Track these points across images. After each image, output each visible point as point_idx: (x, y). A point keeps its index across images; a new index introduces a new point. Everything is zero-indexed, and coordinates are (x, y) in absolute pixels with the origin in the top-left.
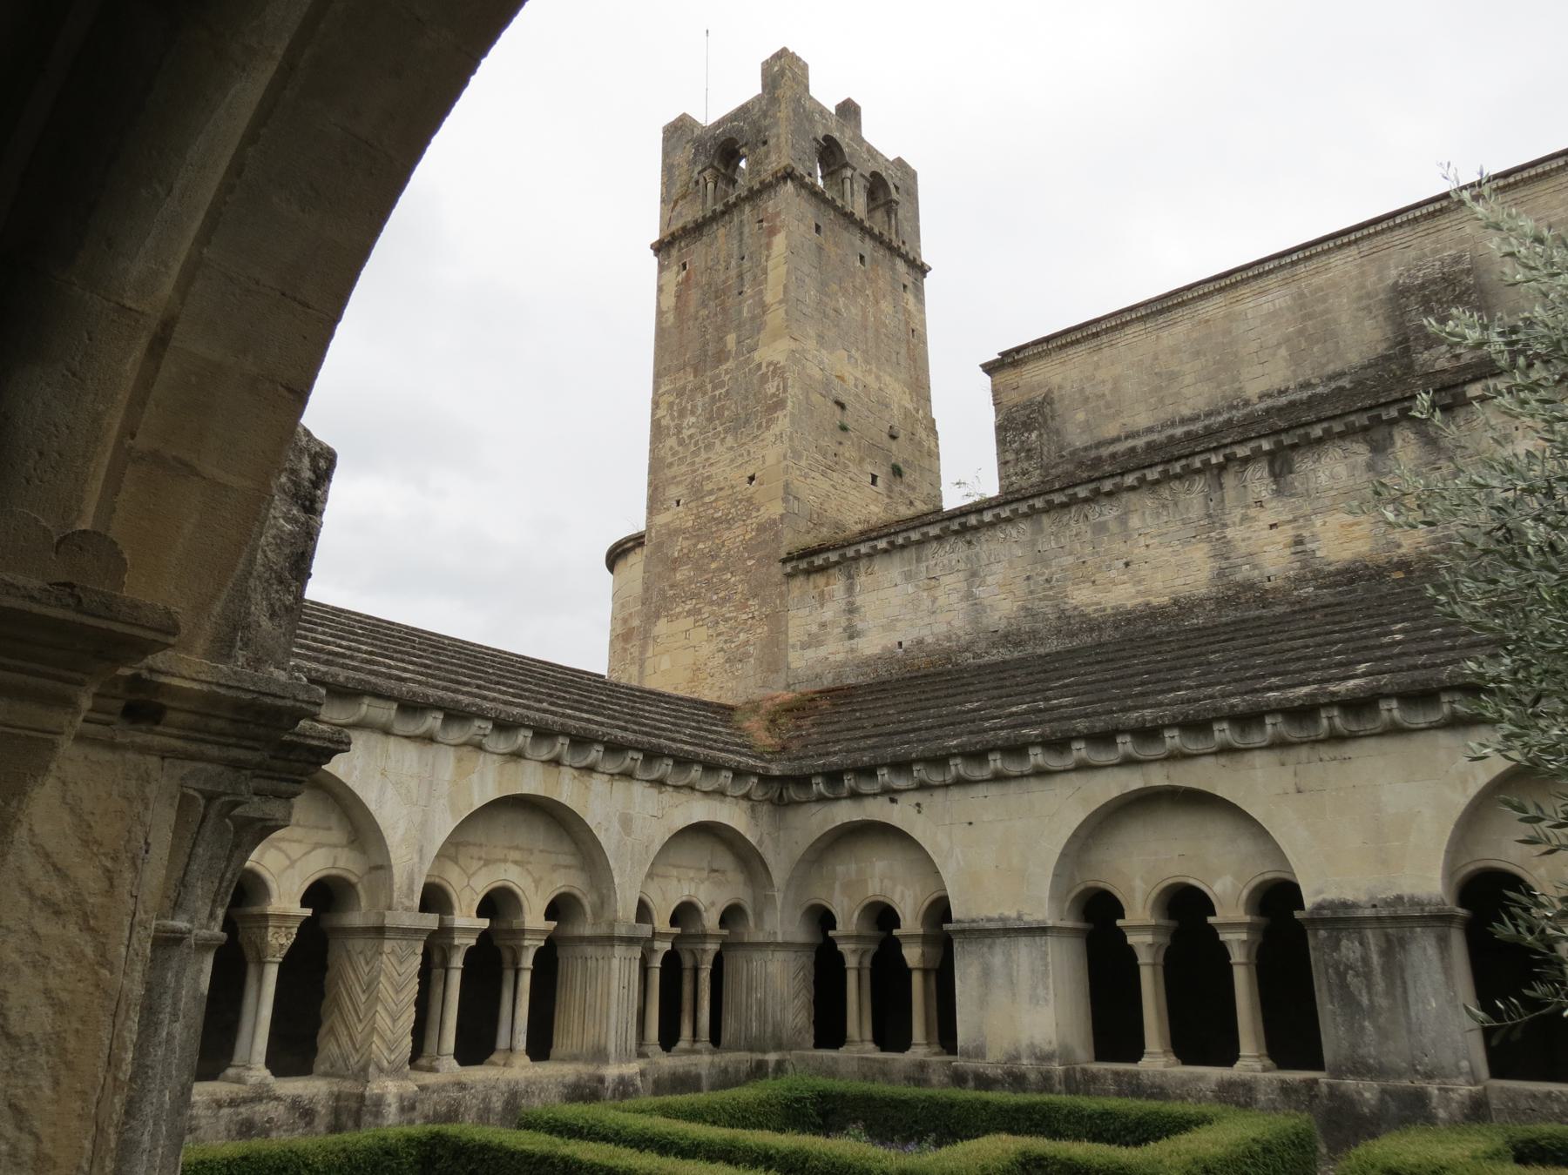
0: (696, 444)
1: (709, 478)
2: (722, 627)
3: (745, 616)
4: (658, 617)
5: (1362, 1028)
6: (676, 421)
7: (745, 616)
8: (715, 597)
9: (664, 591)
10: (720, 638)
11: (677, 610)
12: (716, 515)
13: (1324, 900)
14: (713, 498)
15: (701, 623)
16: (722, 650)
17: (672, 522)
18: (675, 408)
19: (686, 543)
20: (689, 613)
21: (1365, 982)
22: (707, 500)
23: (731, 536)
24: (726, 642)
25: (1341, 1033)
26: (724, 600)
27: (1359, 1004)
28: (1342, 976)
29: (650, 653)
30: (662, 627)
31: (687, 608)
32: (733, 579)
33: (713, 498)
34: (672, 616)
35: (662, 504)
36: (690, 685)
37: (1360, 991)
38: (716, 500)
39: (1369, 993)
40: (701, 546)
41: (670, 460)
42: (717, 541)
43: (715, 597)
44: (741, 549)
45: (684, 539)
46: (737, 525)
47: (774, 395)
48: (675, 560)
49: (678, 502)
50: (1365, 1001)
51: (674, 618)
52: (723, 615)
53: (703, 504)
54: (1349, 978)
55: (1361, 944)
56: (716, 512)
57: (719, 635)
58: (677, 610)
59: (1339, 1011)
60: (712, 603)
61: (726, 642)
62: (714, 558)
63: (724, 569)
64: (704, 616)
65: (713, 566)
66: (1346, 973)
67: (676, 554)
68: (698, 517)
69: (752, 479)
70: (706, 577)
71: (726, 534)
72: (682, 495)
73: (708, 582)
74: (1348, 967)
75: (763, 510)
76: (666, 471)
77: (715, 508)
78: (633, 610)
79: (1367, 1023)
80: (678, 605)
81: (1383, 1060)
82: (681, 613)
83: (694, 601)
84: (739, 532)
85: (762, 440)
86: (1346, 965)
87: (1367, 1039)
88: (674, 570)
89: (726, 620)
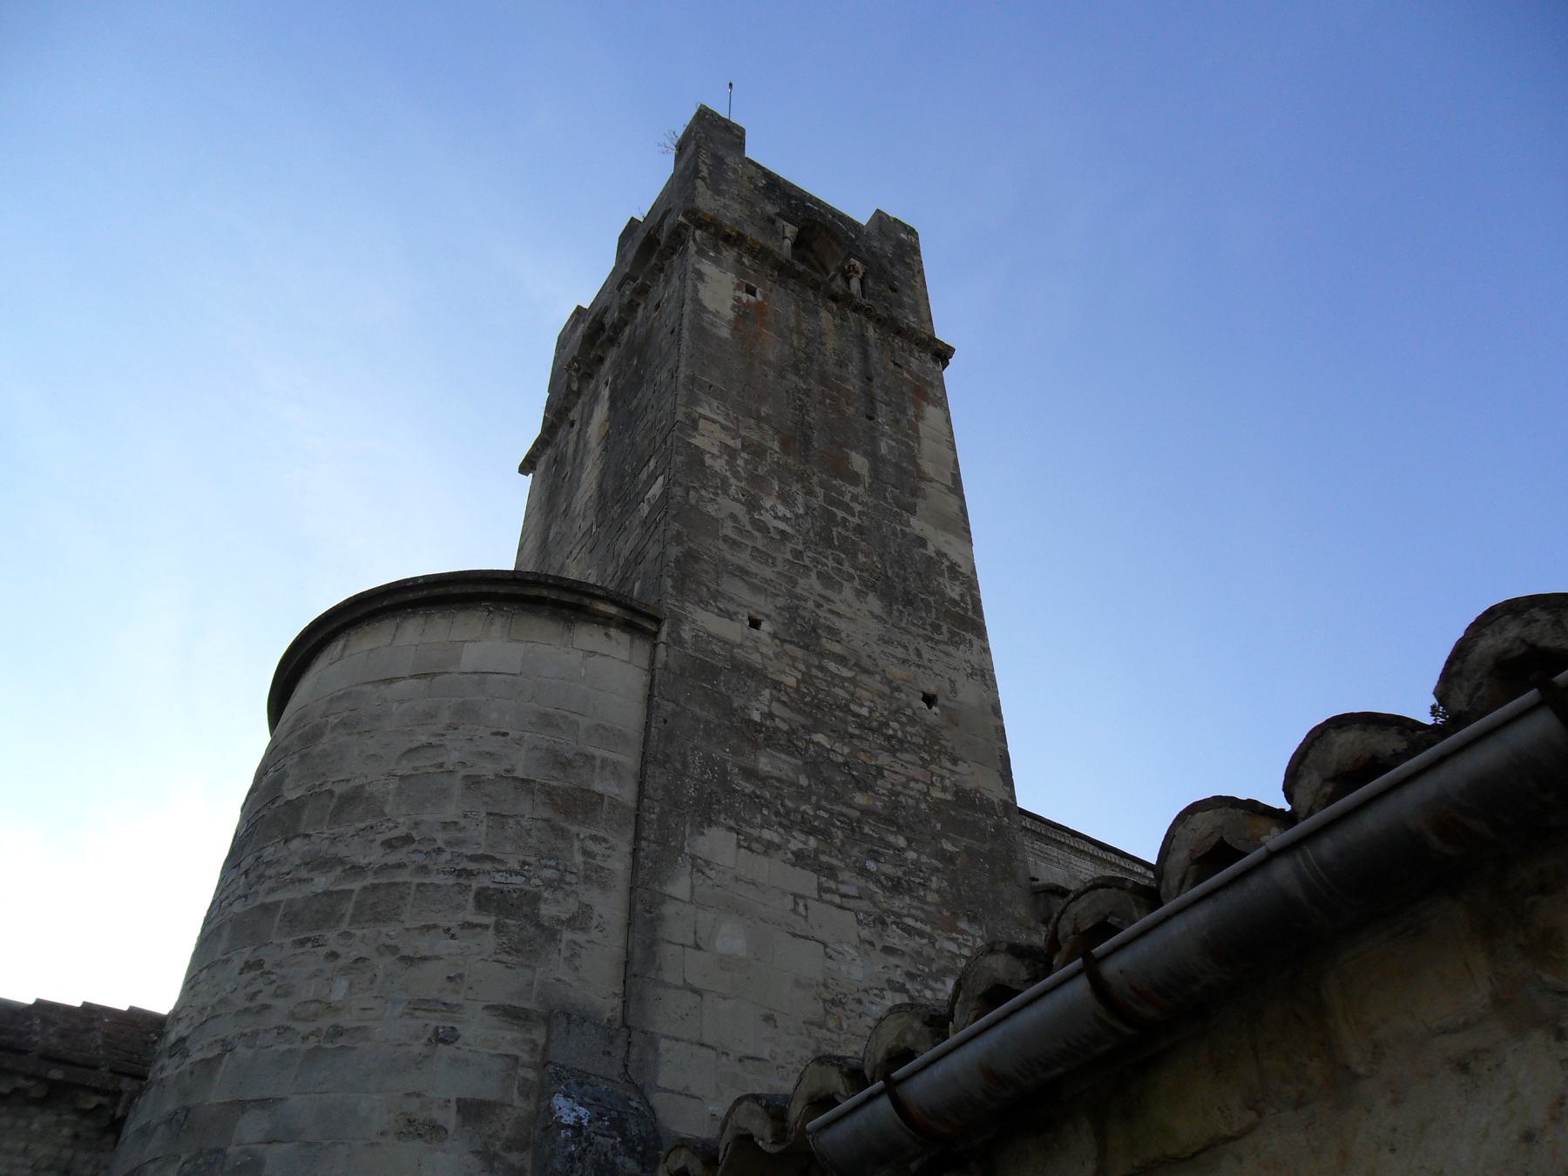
0: (798, 554)
1: (834, 633)
2: (895, 938)
3: (953, 947)
4: (711, 823)
6: (743, 484)
7: (953, 947)
8: (871, 865)
9: (725, 773)
10: (893, 960)
11: (767, 834)
12: (853, 707)
14: (846, 673)
15: (837, 900)
16: (901, 989)
17: (741, 646)
18: (740, 462)
19: (777, 708)
20: (800, 859)
22: (832, 666)
23: (897, 768)
24: (911, 976)
26: (896, 886)
29: (680, 887)
30: (716, 843)
31: (795, 845)
32: (911, 855)
33: (846, 673)
34: (748, 838)
35: (717, 595)
36: (814, 1029)
38: (852, 680)
40: (819, 738)
41: (728, 530)
42: (862, 756)
43: (871, 865)
44: (923, 806)
45: (773, 699)
46: (906, 756)
47: (954, 602)
48: (757, 727)
49: (755, 624)
51: (755, 846)
52: (899, 916)
53: (821, 668)
56: (853, 701)
57: (888, 950)
58: (767, 834)
60: (863, 872)
61: (911, 976)
62: (864, 786)
63: (890, 820)
64: (844, 889)
65: (860, 799)
67: (756, 716)
68: (806, 679)
69: (929, 700)
70: (845, 810)
71: (884, 759)
72: (768, 617)
73: (853, 829)
75: (962, 768)
76: (720, 544)
77: (852, 695)
78: (600, 753)
80: (766, 824)
82: (779, 847)
83: (812, 842)
84: (916, 772)
85: (946, 654)
88: (756, 747)
89: (909, 930)
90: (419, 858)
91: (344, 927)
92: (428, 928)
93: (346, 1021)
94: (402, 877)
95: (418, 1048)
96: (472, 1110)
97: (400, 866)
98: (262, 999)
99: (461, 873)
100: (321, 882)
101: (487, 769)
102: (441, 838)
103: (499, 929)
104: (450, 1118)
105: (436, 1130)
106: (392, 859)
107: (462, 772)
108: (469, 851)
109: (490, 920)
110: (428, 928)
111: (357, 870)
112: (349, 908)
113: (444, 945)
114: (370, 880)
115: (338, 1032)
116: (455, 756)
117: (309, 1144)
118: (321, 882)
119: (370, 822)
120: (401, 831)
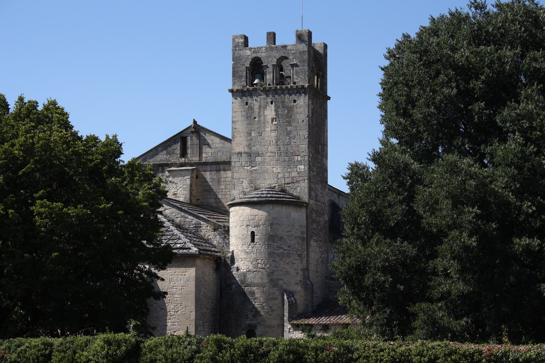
90: (292, 249)
91: (285, 258)
92: (294, 259)
93: (288, 270)
94: (291, 252)
95: (296, 275)
96: (300, 281)
97: (290, 250)
98: (277, 266)
99: (296, 252)
100: (281, 251)
101: (296, 235)
102: (294, 246)
103: (300, 259)
104: (299, 283)
105: (298, 284)
106: (289, 249)
107: (294, 236)
108: (296, 248)
109: (299, 258)
110: (294, 259)
111: (285, 250)
112: (285, 255)
113: (296, 262)
114: (287, 252)
115: (287, 272)
116: (293, 233)
117: (287, 285)
118: (281, 251)
119: (285, 242)
120: (289, 245)
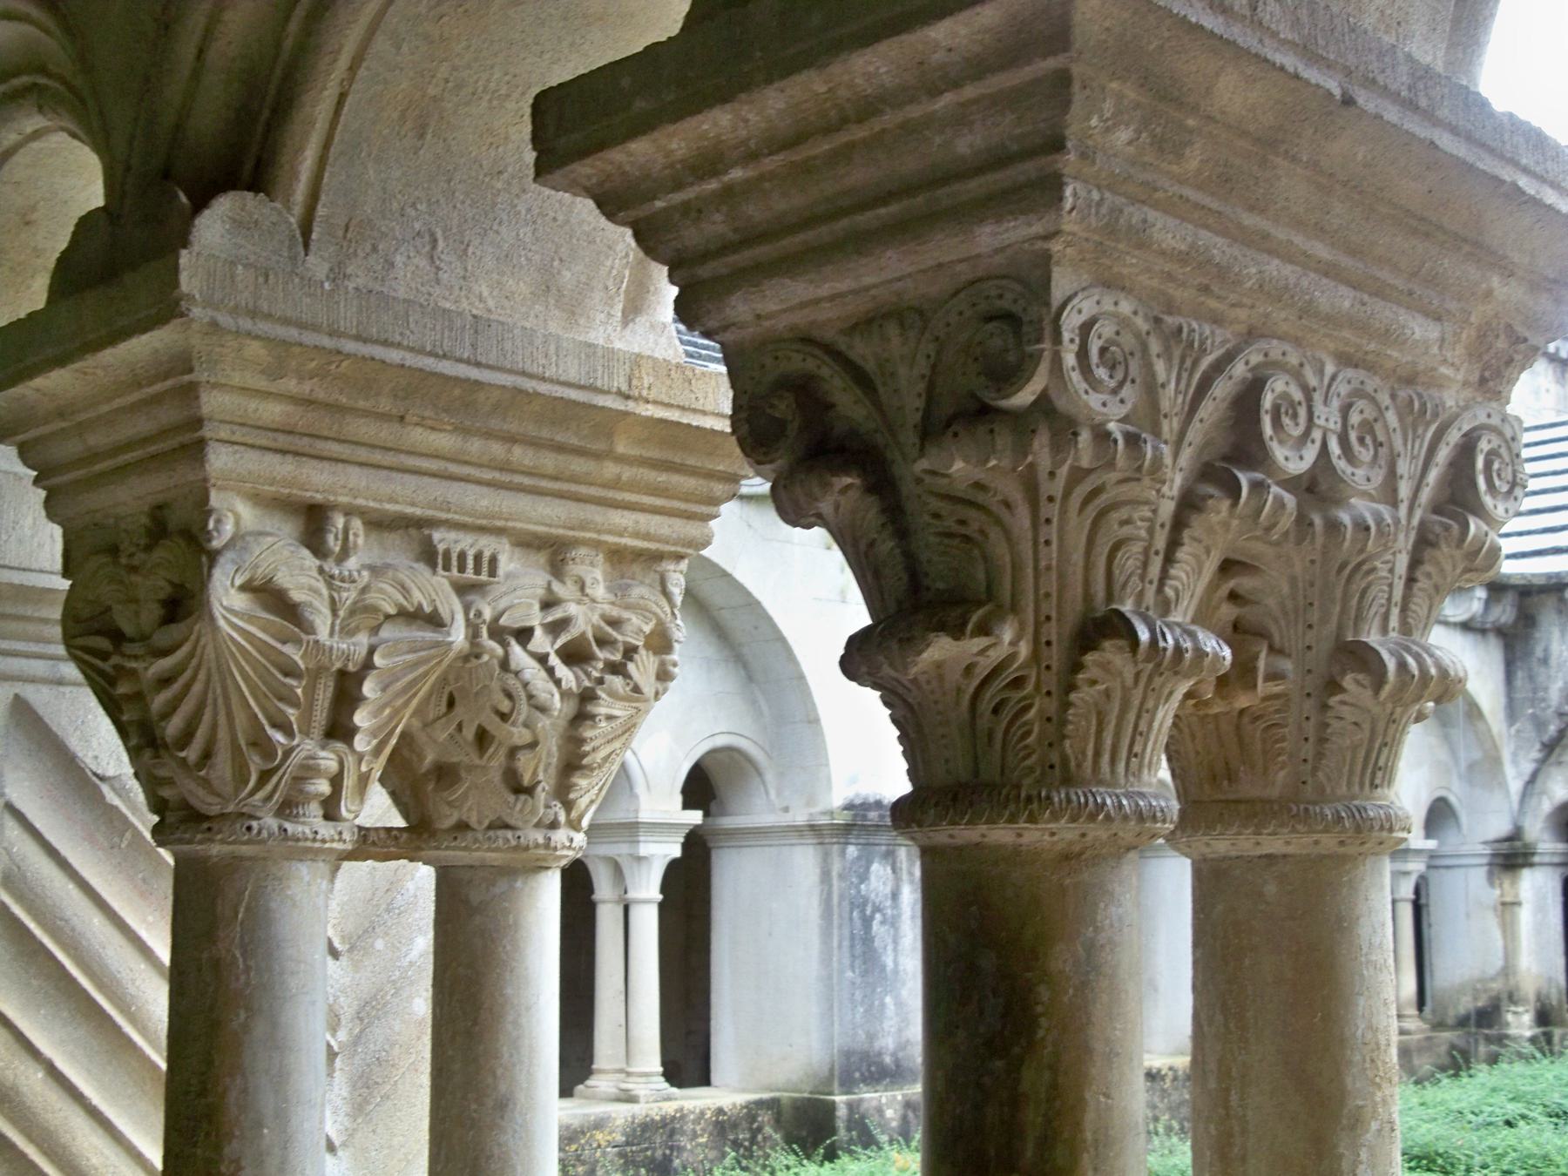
5: (883, 1005)
13: (857, 795)
21: (892, 932)
25: (858, 1016)
27: (883, 968)
28: (867, 922)
37: (885, 948)
39: (895, 950)
50: (889, 961)
54: (875, 925)
55: (894, 871)
59: (858, 981)
66: (872, 918)
74: (877, 909)
79: (888, 1000)
81: (901, 1055)
86: (874, 903)
87: (887, 1025)
